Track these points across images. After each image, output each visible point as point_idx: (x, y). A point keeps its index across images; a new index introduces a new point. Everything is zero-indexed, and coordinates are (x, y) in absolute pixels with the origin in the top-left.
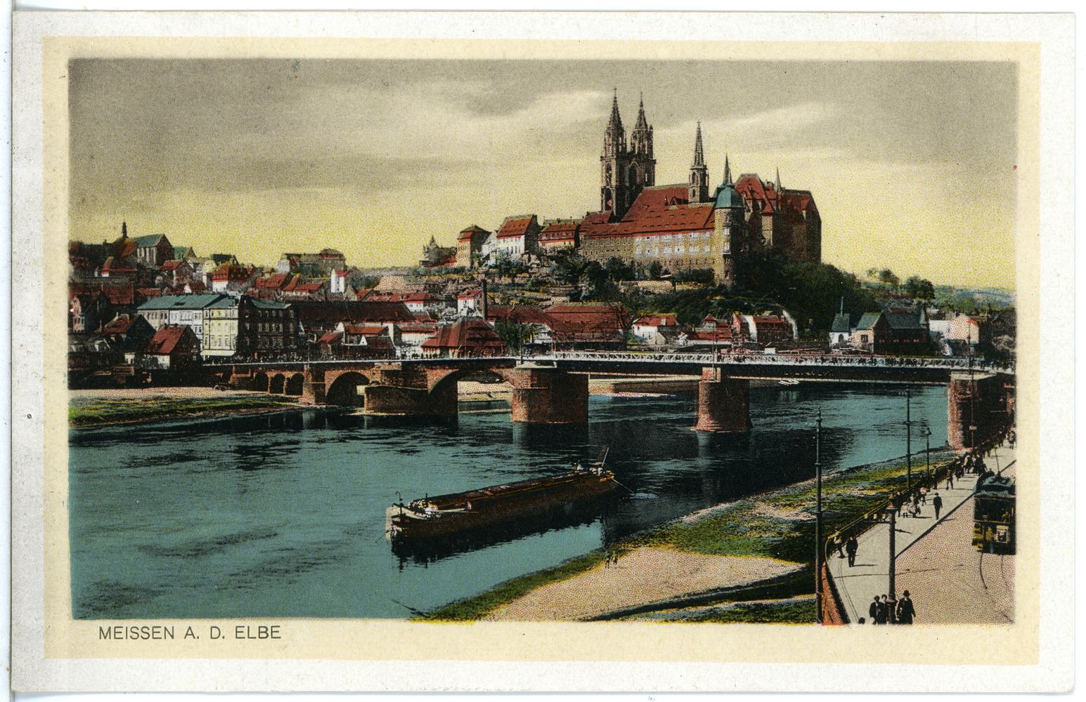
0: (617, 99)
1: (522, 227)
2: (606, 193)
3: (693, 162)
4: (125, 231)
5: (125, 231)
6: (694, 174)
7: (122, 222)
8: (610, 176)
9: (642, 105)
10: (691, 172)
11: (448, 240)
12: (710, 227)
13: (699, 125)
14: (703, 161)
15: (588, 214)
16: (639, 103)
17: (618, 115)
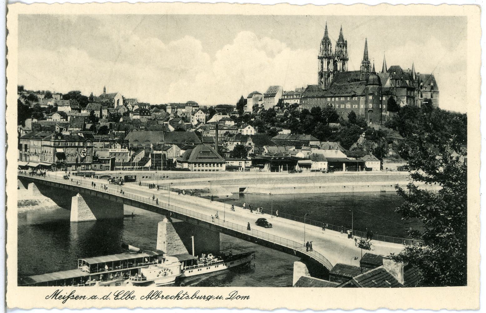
1: (275, 92)
2: (321, 74)
3: (363, 59)
4: (105, 91)
5: (105, 91)
6: (363, 65)
7: (104, 86)
9: (341, 30)
10: (362, 64)
11: (245, 97)
12: (364, 94)
13: (366, 40)
14: (368, 59)
16: (340, 29)
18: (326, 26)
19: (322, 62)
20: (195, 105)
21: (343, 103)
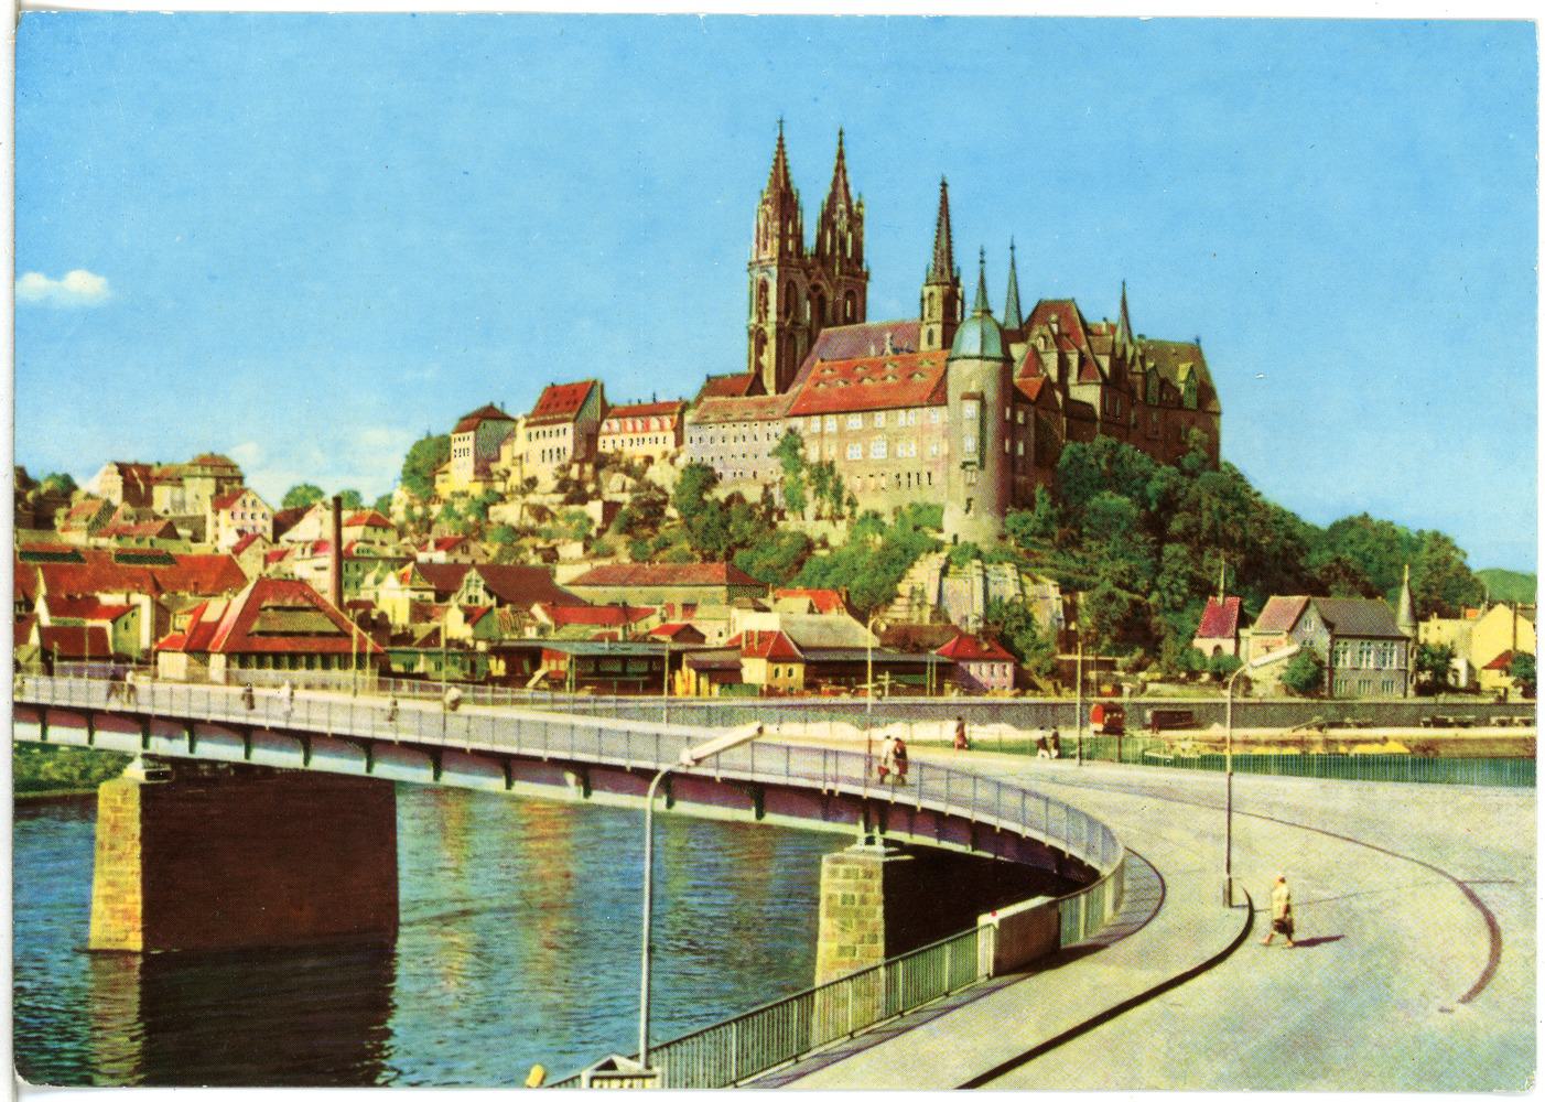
0: (785, 142)
6: (931, 294)
8: (766, 303)
9: (841, 156)
10: (927, 291)
14: (951, 270)
15: (709, 379)
17: (786, 175)
18: (781, 139)
19: (764, 287)
20: (228, 472)
21: (857, 436)
